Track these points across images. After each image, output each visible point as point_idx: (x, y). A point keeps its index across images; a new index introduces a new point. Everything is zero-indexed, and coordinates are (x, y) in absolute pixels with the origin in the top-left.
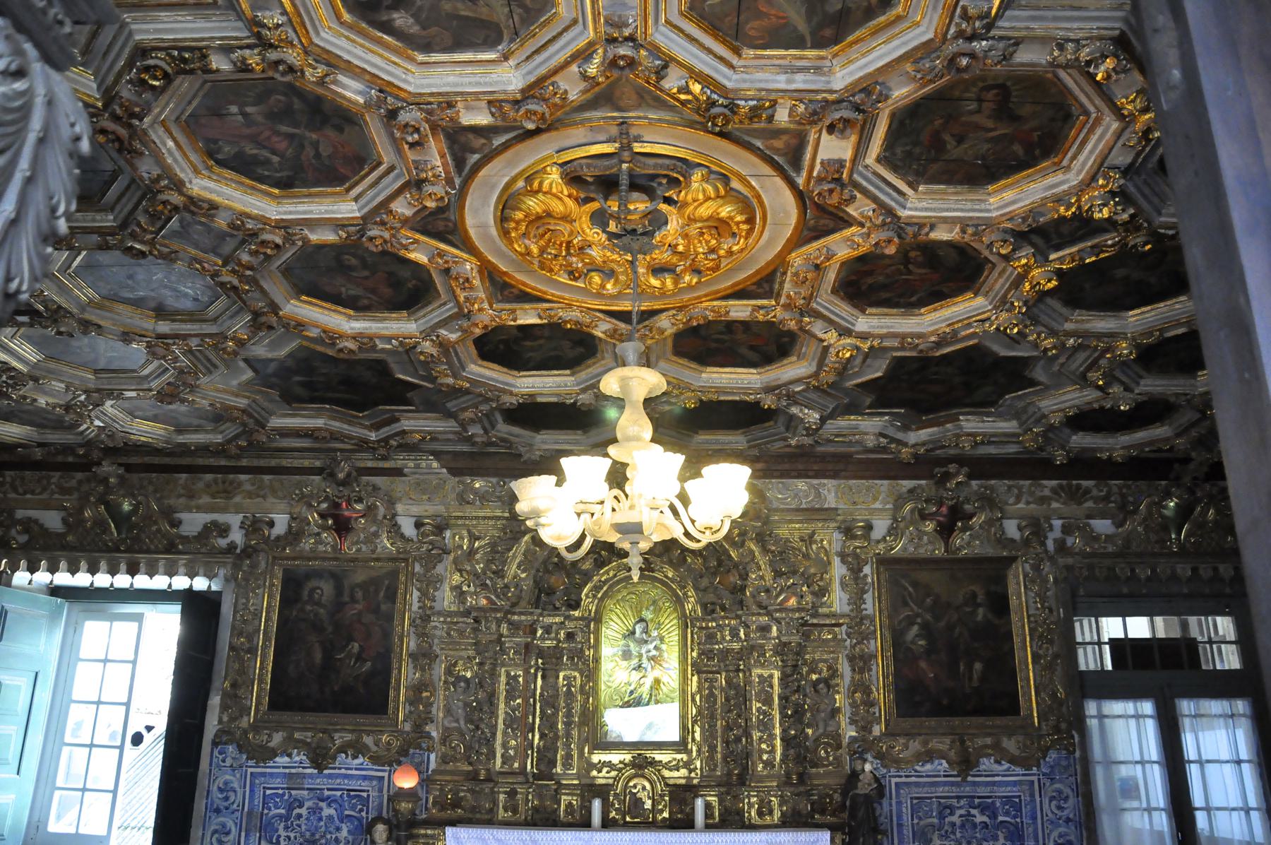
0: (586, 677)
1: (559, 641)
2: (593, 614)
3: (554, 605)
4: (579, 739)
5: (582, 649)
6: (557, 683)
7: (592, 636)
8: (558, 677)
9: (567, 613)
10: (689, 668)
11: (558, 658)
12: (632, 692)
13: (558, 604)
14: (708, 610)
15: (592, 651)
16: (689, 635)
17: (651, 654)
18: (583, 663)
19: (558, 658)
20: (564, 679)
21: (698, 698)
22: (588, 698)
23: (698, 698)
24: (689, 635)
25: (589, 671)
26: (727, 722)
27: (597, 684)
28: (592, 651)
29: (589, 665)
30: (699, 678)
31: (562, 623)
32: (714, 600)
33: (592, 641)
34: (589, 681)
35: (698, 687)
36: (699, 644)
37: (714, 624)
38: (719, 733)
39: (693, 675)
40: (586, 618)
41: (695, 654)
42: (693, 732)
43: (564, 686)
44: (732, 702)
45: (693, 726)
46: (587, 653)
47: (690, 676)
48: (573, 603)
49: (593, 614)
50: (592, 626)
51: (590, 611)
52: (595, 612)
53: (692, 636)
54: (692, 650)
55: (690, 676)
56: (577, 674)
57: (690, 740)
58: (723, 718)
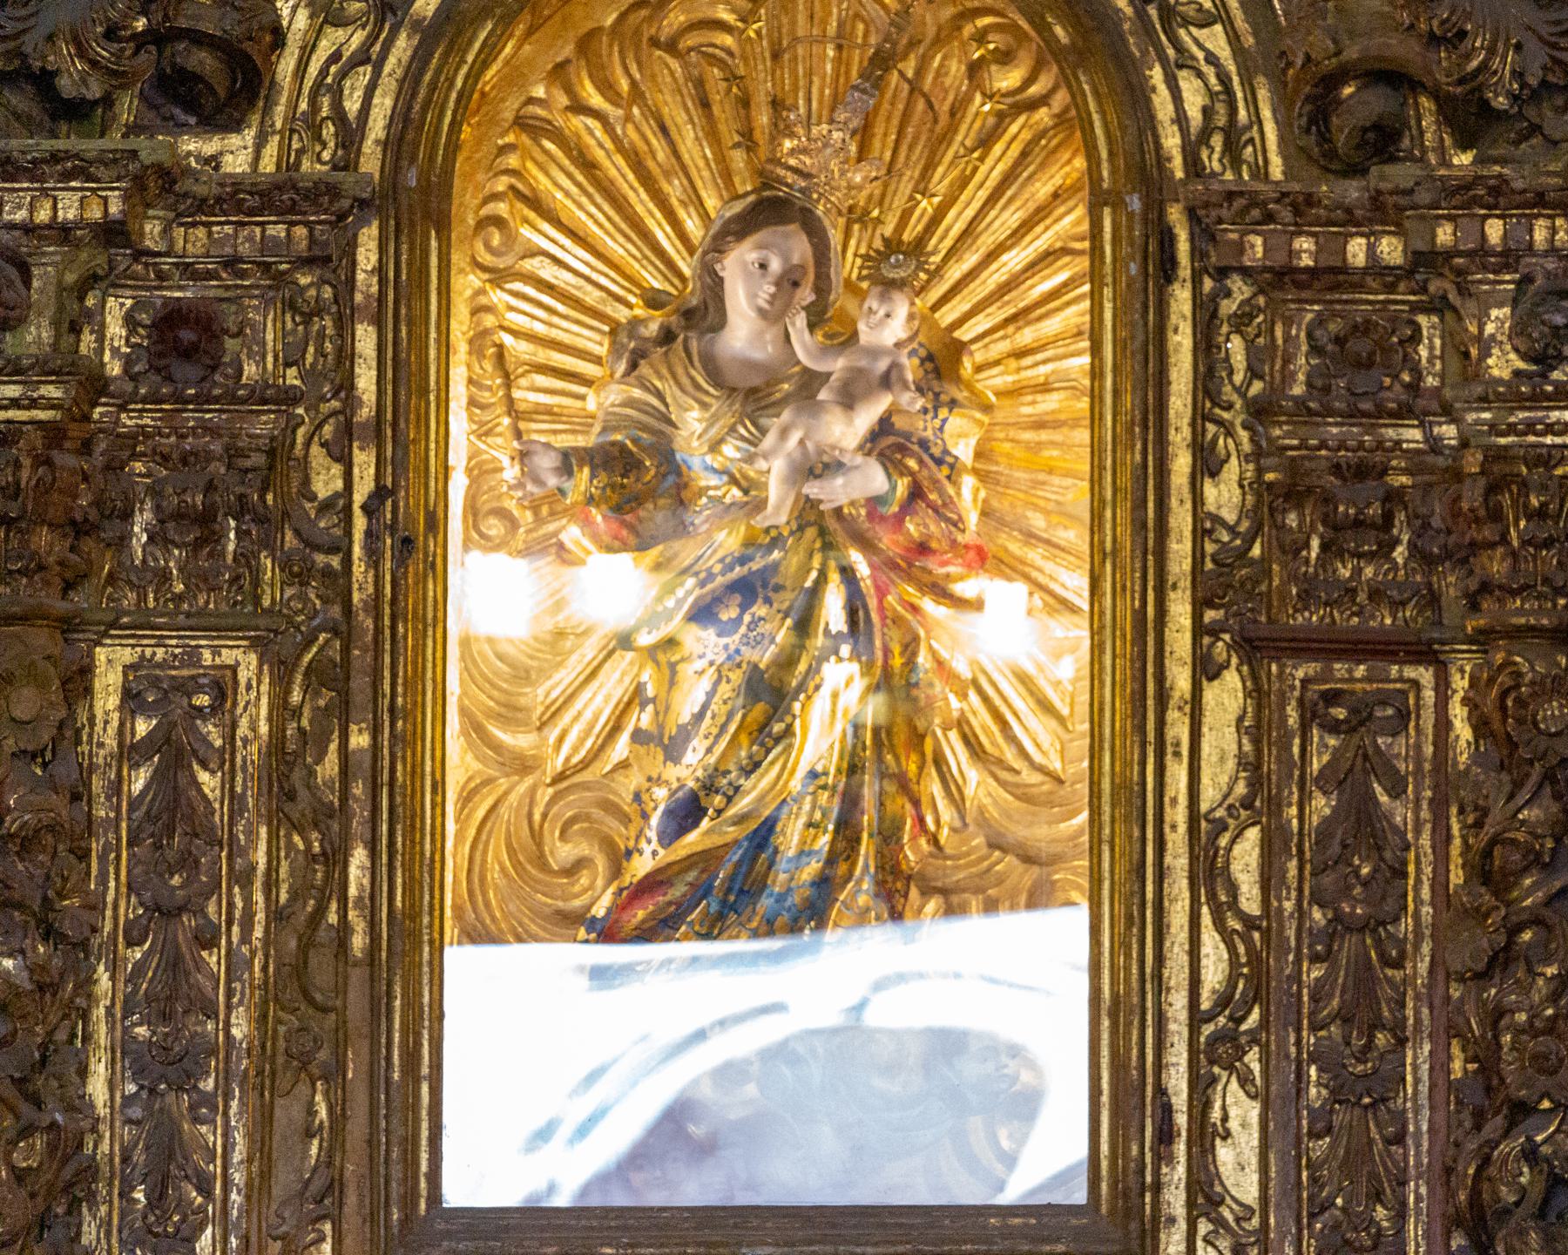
0: (318, 676)
1: (95, 385)
2: (371, 161)
3: (44, 82)
4: (258, 1189)
5: (278, 451)
6: (68, 732)
7: (365, 339)
8: (79, 682)
9: (150, 149)
10: (1180, 610)
11: (80, 529)
12: (687, 812)
13: (73, 78)
14: (1343, 131)
15: (364, 461)
16: (1182, 341)
17: (836, 492)
18: (297, 573)
19: (80, 529)
20: (132, 700)
21: (1245, 856)
22: (336, 858)
23: (1245, 856)
24: (1182, 341)
25: (344, 631)
26: (1486, 1061)
27: (406, 741)
28: (364, 461)
29: (338, 582)
30: (1257, 692)
31: (113, 233)
32: (1404, 50)
33: (366, 381)
34: (343, 712)
35: (1251, 766)
36: (1260, 412)
37: (1391, 249)
38: (1418, 1153)
39: (1205, 669)
40: (322, 193)
41: (1224, 496)
42: (1205, 1136)
43: (131, 753)
44: (1530, 892)
45: (1201, 1088)
46: (325, 482)
47: (1181, 679)
48: (203, 61)
49: (371, 161)
50: (367, 256)
51: (350, 135)
52: (397, 145)
53: (1206, 345)
54: (1207, 464)
55: (1181, 679)
56: (248, 664)
57: (1176, 1200)
58: (1451, 1029)
